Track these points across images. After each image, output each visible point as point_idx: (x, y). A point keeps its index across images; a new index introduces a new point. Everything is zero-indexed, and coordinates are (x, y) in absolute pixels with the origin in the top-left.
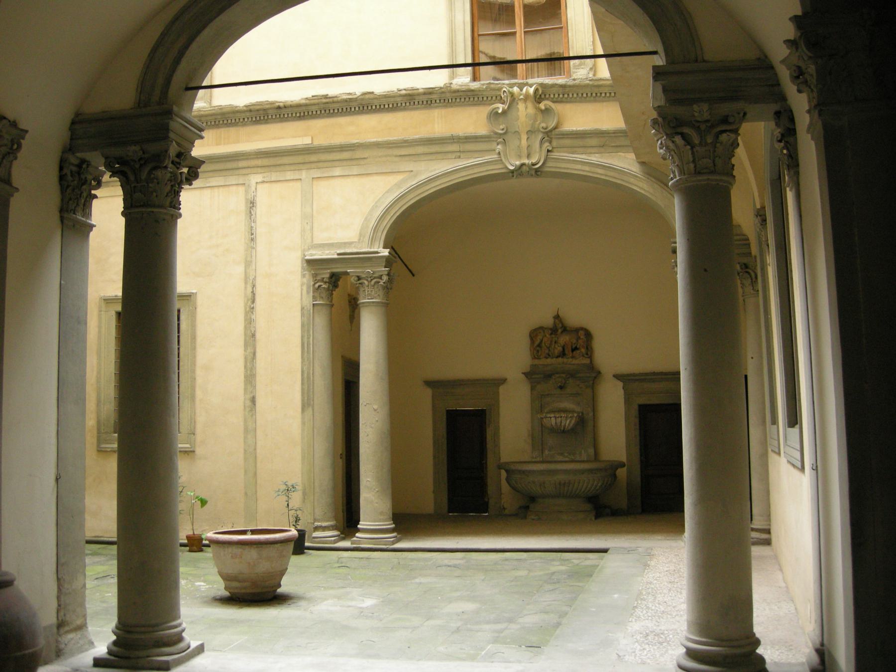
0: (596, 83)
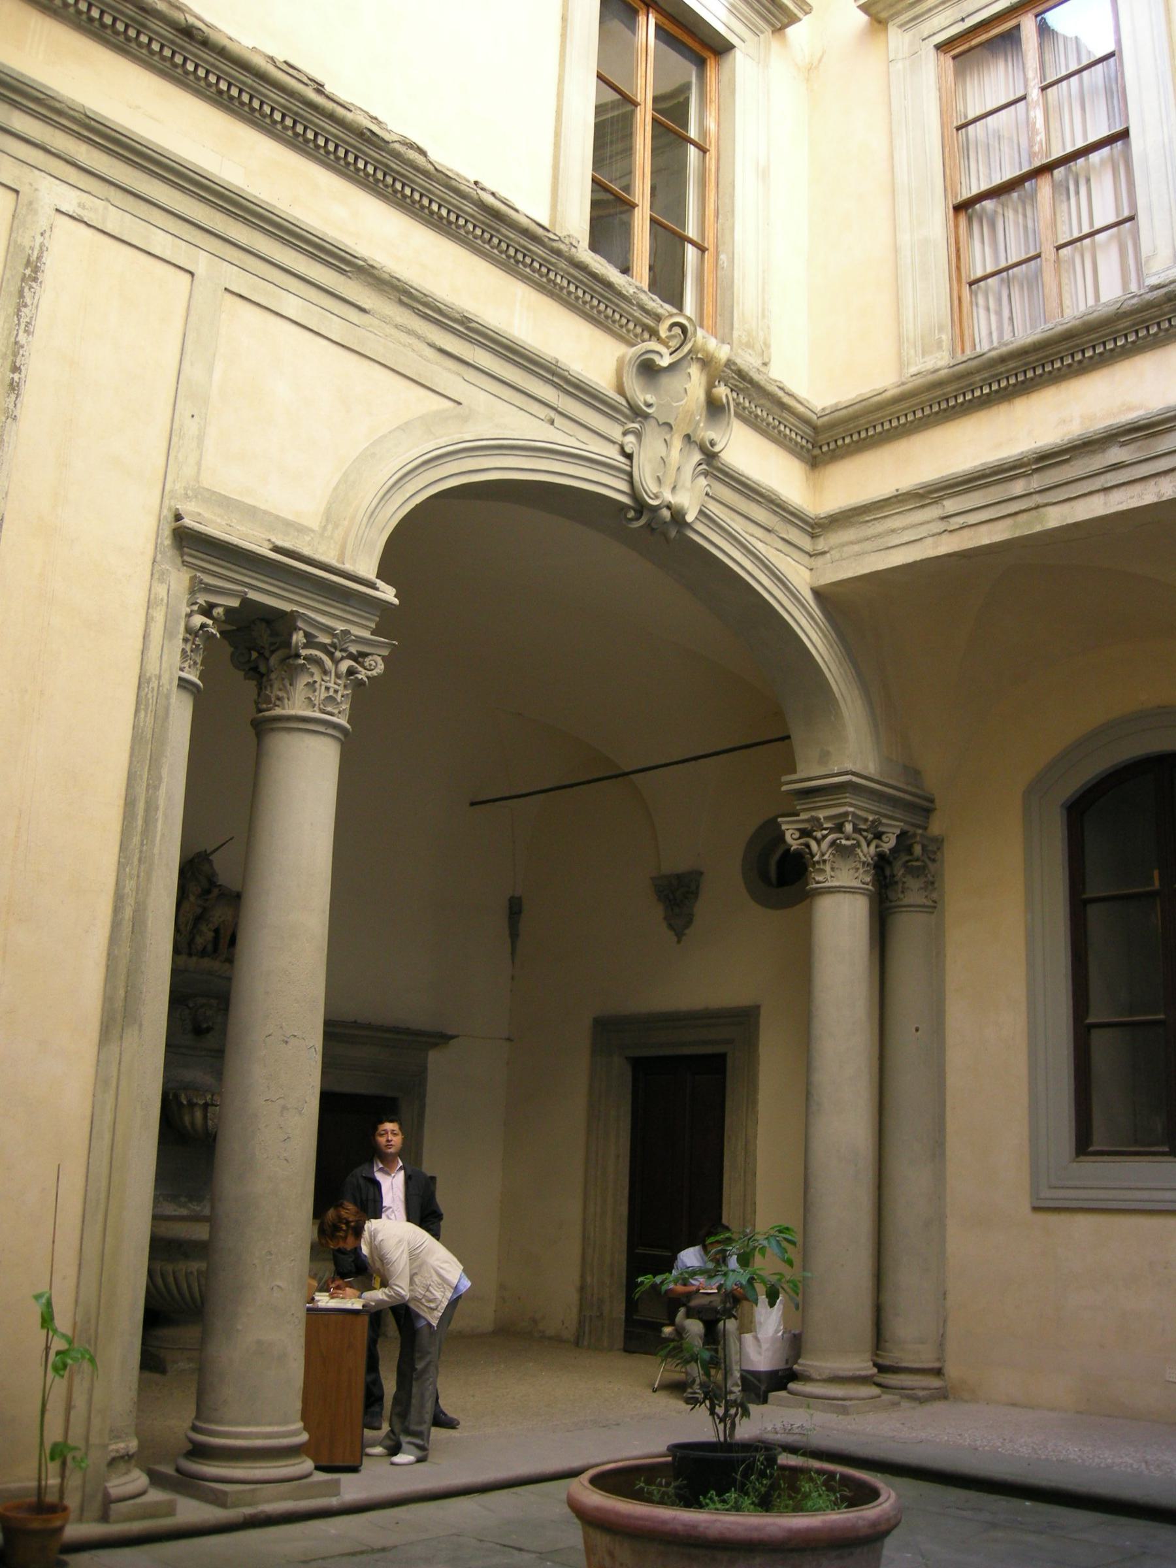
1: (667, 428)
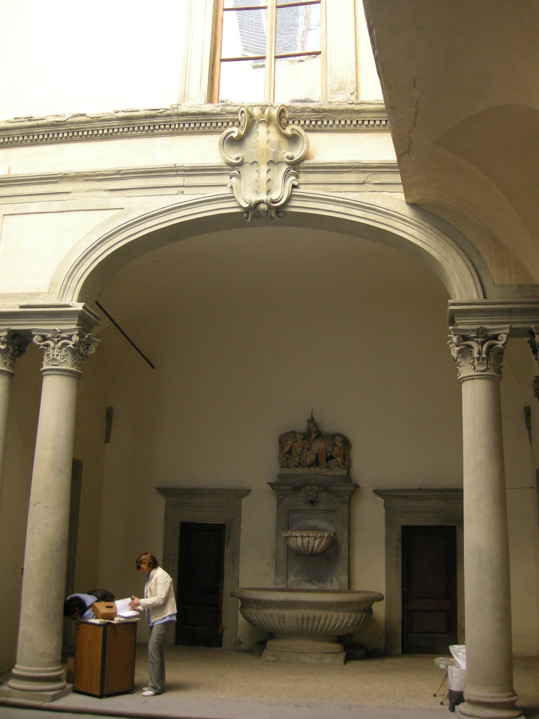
0: (358, 107)
1: (255, 164)
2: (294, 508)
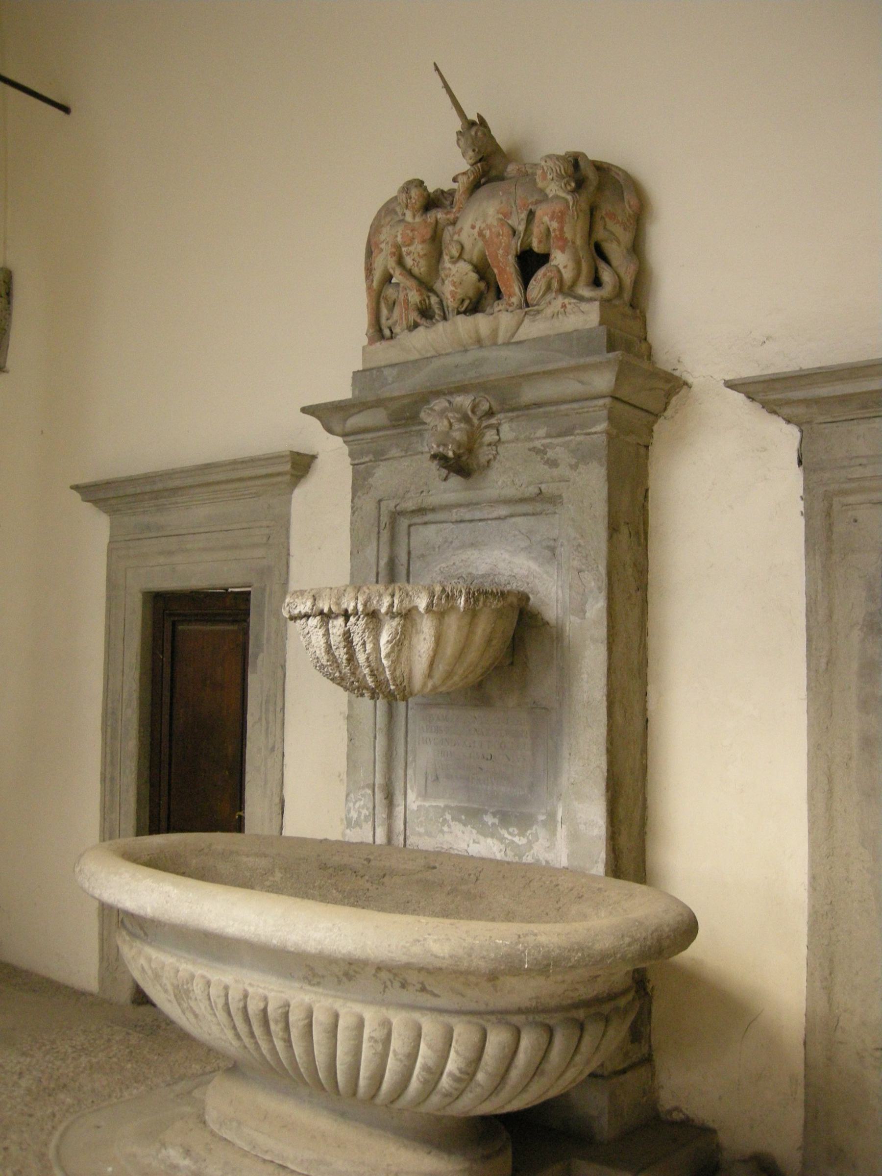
2: (410, 505)
